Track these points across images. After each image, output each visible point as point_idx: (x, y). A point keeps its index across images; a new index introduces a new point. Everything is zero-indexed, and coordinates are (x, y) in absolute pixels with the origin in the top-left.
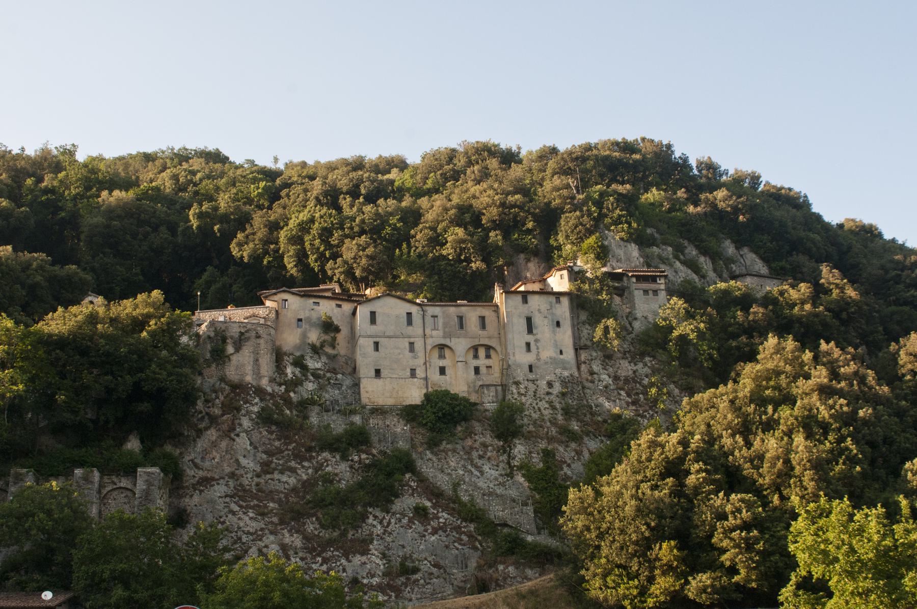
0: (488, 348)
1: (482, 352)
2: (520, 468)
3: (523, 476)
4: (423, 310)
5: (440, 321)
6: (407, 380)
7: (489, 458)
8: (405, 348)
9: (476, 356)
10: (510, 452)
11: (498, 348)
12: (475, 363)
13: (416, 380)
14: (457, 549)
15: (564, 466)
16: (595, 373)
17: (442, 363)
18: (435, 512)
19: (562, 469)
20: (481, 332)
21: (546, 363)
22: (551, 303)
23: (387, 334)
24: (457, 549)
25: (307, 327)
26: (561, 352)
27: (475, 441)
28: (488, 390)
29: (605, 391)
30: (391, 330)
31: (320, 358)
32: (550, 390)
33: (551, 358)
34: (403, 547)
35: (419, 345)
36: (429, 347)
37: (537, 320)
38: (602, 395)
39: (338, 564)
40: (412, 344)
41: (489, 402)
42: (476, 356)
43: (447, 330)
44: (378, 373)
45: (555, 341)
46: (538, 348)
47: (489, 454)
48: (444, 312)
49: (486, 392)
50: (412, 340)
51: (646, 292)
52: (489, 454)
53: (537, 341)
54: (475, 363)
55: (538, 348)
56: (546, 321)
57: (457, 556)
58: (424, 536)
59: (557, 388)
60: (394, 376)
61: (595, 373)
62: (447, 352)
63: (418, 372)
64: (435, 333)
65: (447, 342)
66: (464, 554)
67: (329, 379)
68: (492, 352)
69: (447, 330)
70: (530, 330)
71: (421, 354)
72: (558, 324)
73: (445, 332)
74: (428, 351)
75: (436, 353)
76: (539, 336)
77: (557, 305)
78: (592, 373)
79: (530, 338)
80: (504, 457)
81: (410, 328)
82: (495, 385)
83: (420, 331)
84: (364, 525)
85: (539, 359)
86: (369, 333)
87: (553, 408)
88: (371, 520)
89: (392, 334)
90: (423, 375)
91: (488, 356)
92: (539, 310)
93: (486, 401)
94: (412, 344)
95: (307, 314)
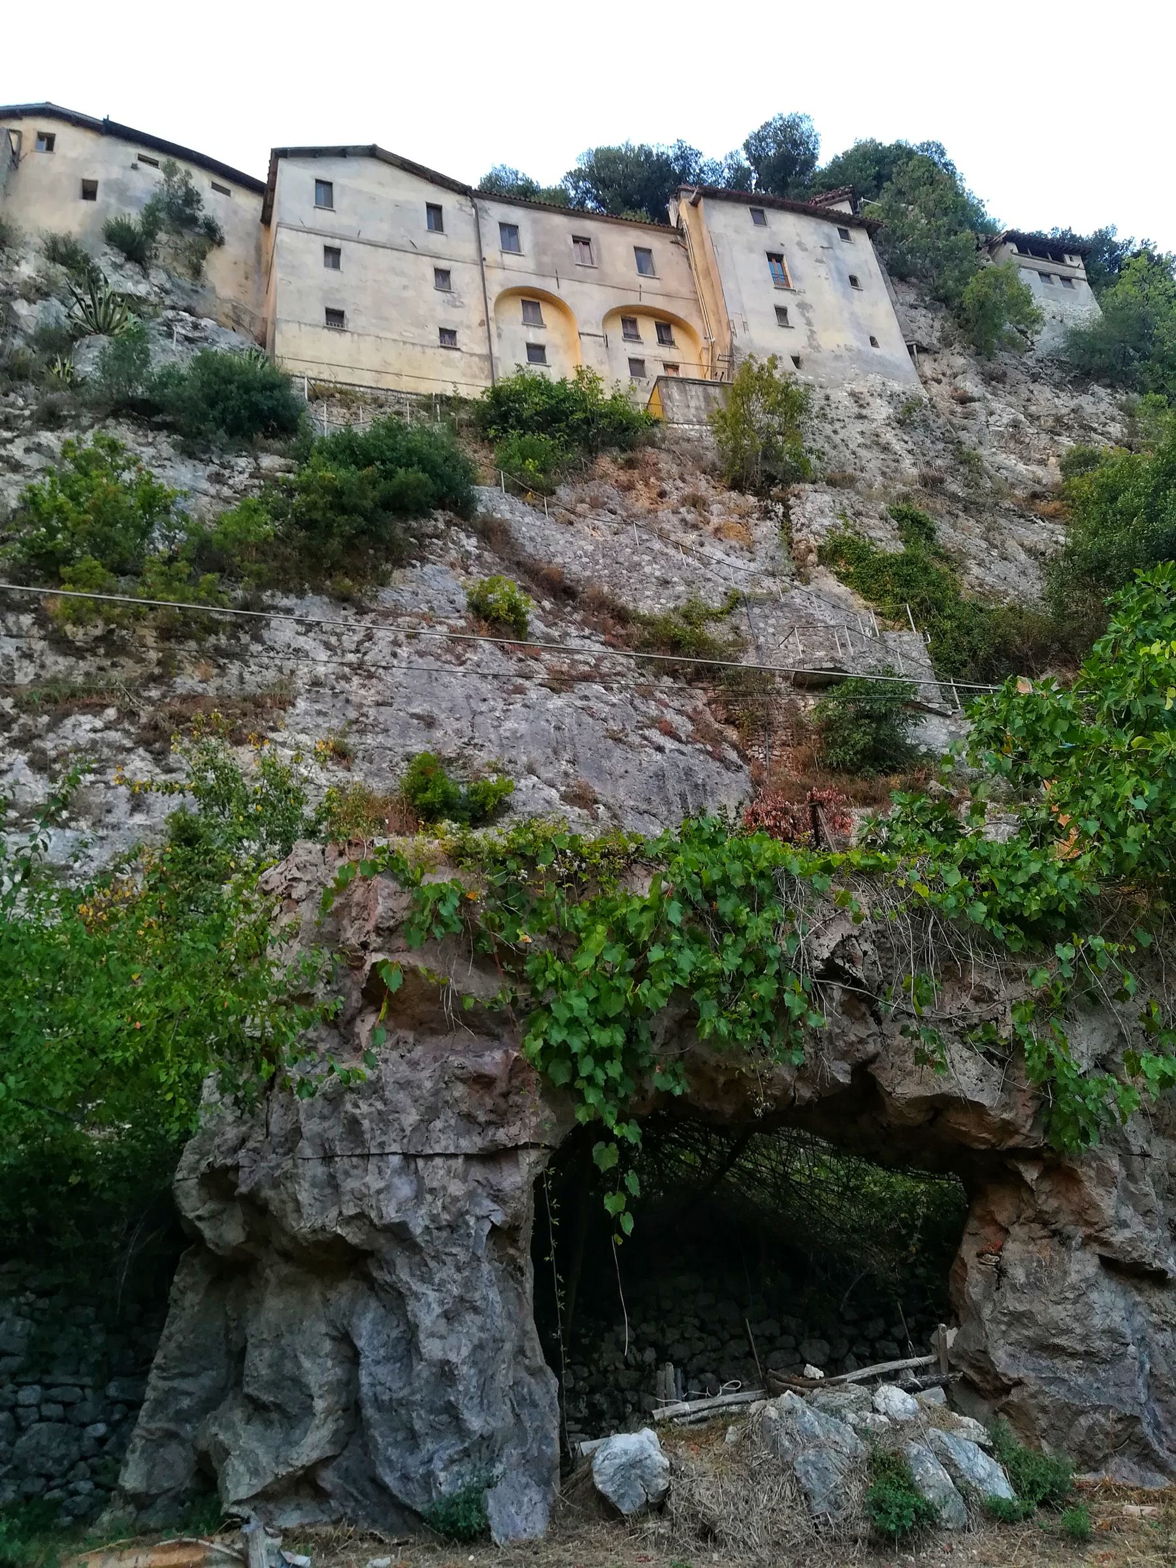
0: (666, 325)
1: (647, 329)
2: (830, 555)
3: (843, 578)
4: (474, 206)
5: (526, 238)
6: (429, 351)
7: (717, 530)
8: (423, 278)
9: (632, 336)
10: (786, 515)
11: (695, 323)
12: (633, 350)
13: (457, 354)
14: (660, 749)
15: (971, 564)
16: (972, 400)
17: (534, 336)
18: (556, 633)
19: (967, 570)
20: (641, 280)
21: (837, 358)
22: (829, 238)
23: (366, 235)
24: (660, 749)
25: (113, 201)
26: (873, 342)
27: (662, 494)
28: (683, 392)
29: (1013, 436)
30: (379, 230)
31: (146, 276)
32: (864, 412)
33: (849, 349)
34: (429, 722)
35: (464, 277)
36: (495, 290)
37: (796, 261)
38: (1004, 448)
39: (112, 776)
40: (442, 275)
41: (689, 422)
42: (632, 336)
43: (546, 259)
44: (335, 317)
45: (852, 314)
46: (809, 323)
47: (715, 521)
48: (535, 222)
49: (676, 395)
50: (443, 265)
51: (1045, 275)
52: (715, 521)
53: (803, 306)
54: (633, 350)
55: (809, 323)
56: (822, 270)
57: (660, 776)
58: (520, 690)
59: (881, 411)
60: (389, 335)
61: (972, 400)
62: (547, 313)
63: (461, 337)
64: (509, 259)
65: (548, 285)
66: (689, 772)
67: (168, 324)
68: (676, 334)
69: (546, 259)
70: (782, 282)
71: (472, 299)
72: (853, 281)
73: (539, 264)
74: (491, 305)
75: (514, 310)
76: (808, 298)
77: (845, 245)
78: (964, 400)
79: (784, 299)
80: (766, 529)
81: (436, 237)
82: (702, 383)
83: (470, 250)
84: (256, 648)
85: (817, 348)
86: (308, 224)
87: (886, 448)
88: (283, 631)
89: (381, 238)
90: (484, 350)
91: (665, 339)
92: (799, 244)
93: (678, 417)
94: (442, 275)
95: (116, 173)
